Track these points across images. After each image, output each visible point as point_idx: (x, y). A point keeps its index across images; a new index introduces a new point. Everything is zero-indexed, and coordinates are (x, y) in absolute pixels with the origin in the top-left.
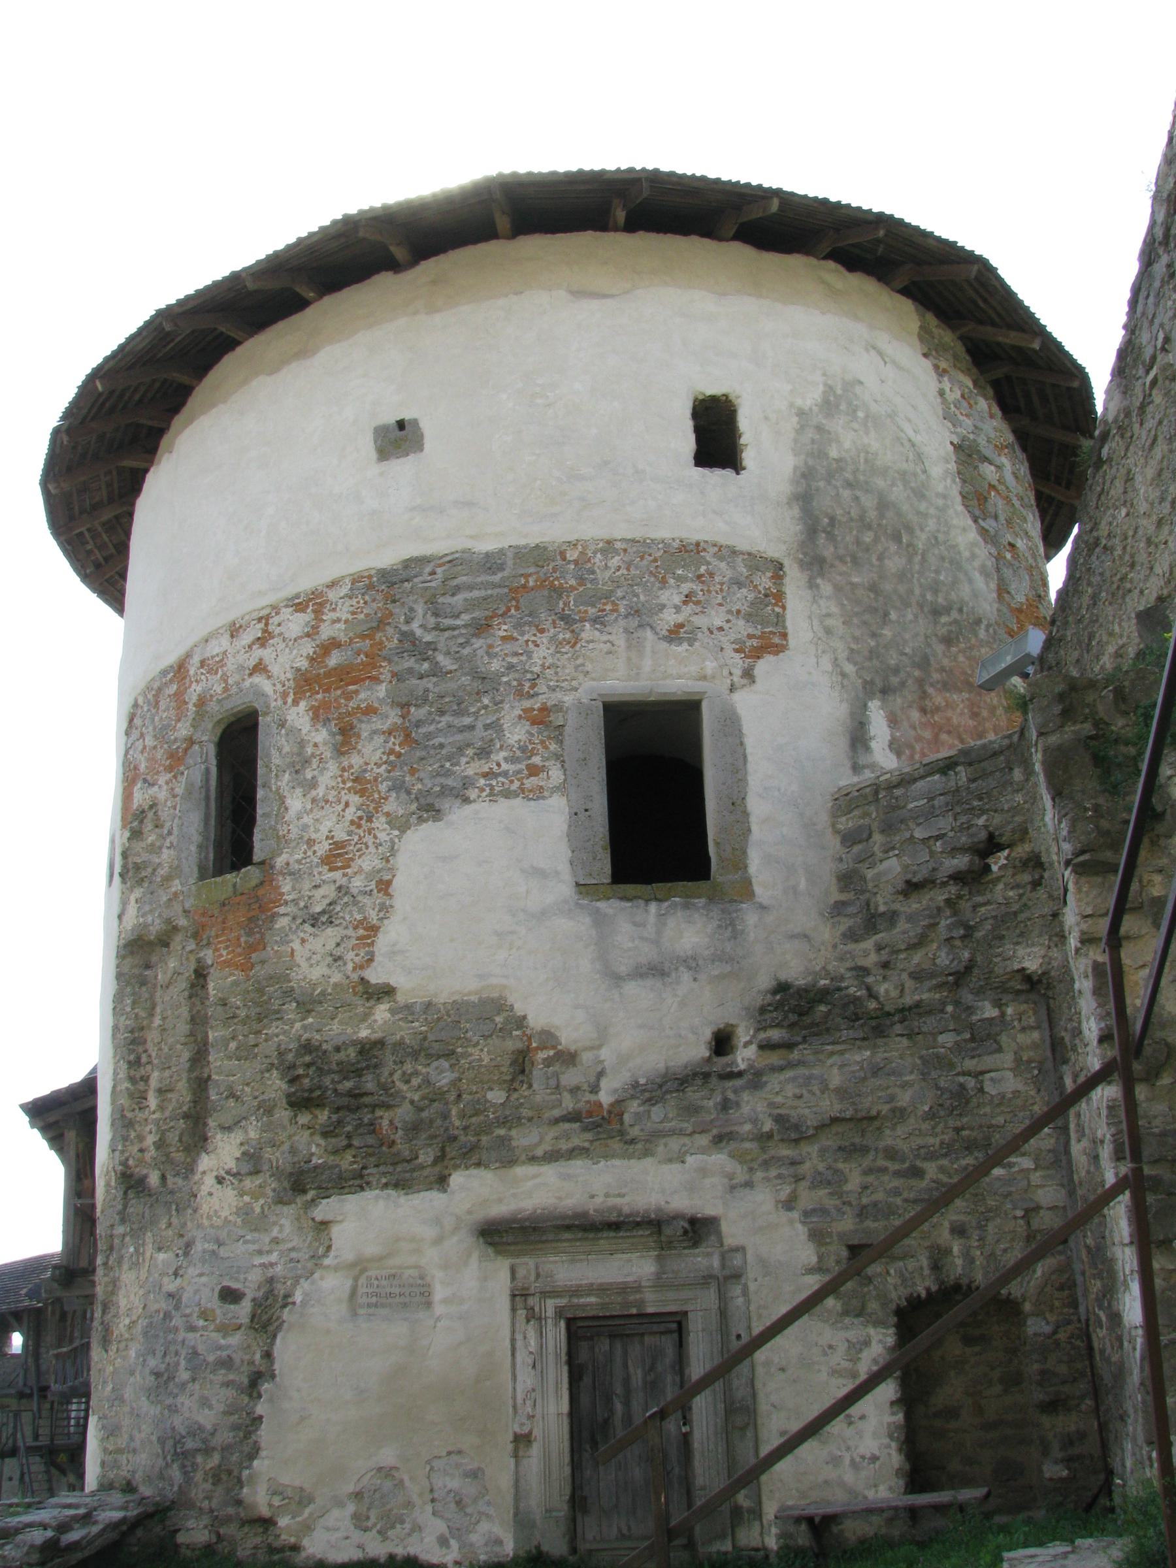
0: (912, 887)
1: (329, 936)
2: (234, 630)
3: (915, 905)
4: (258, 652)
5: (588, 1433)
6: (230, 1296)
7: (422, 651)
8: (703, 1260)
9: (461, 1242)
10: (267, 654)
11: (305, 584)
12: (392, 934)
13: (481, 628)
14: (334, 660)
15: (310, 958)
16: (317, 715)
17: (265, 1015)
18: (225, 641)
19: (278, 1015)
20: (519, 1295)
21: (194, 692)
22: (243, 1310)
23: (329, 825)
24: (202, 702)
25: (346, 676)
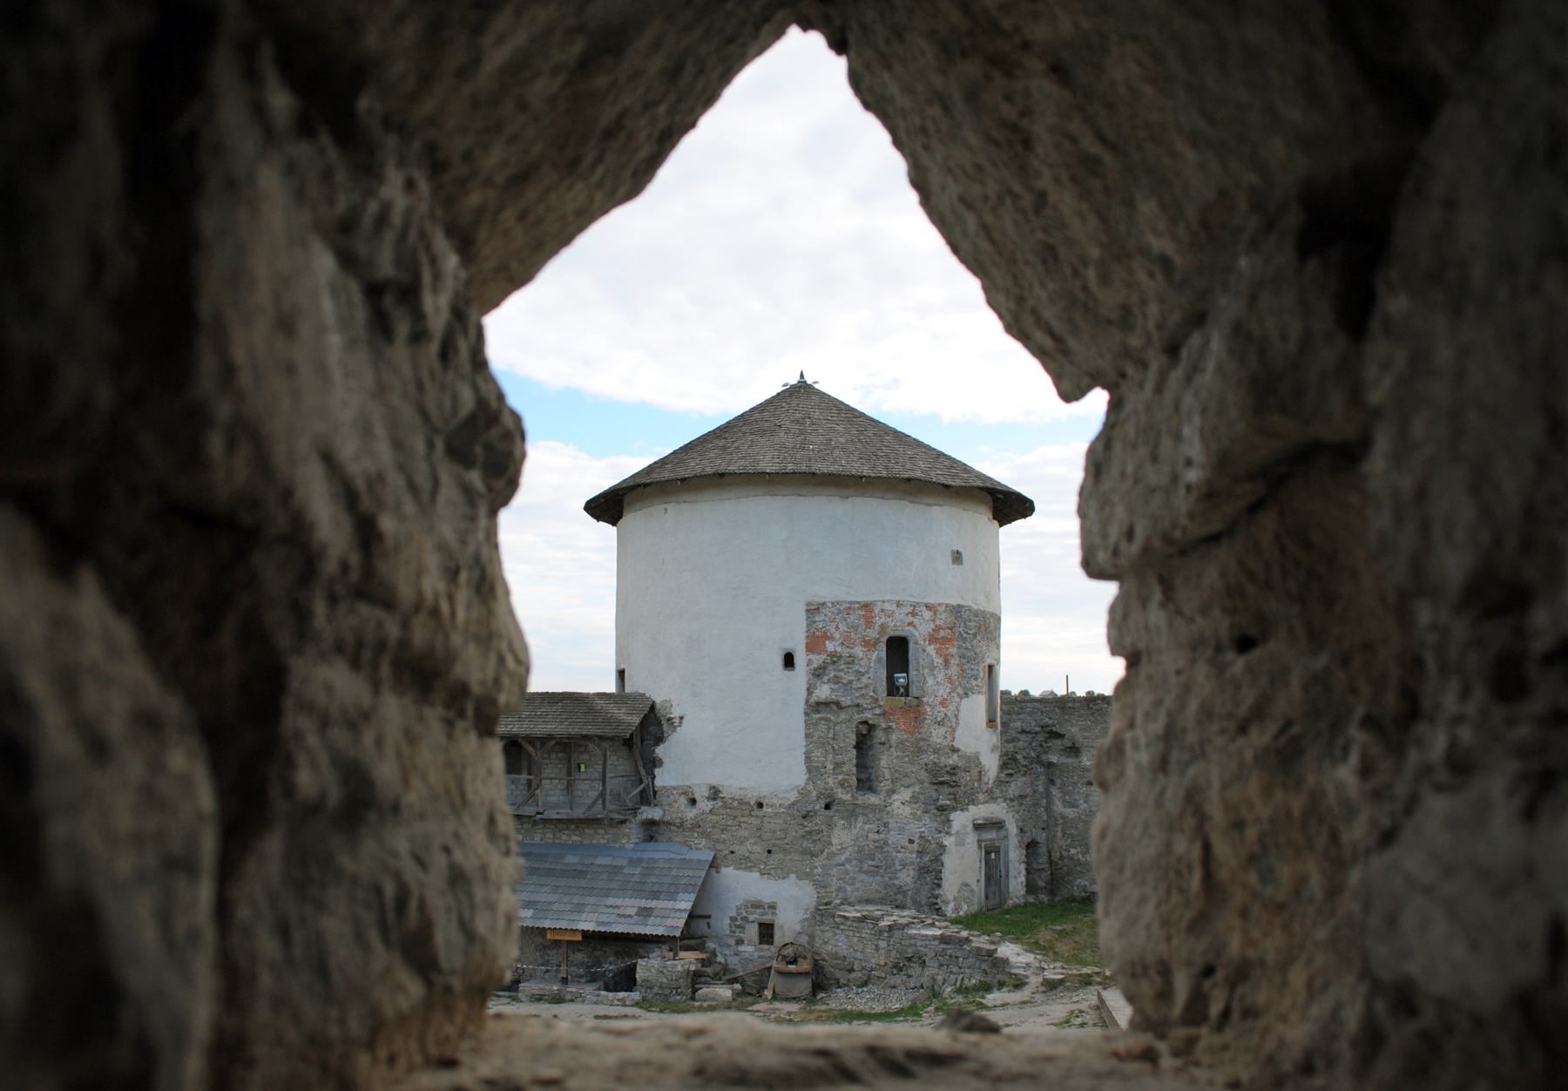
0: (1023, 732)
1: (943, 729)
2: (899, 604)
3: (1023, 737)
4: (910, 619)
5: (988, 878)
6: (911, 842)
7: (964, 640)
8: (1002, 833)
9: (970, 828)
10: (916, 620)
11: (930, 600)
12: (959, 732)
13: (975, 635)
14: (942, 633)
15: (937, 735)
16: (938, 651)
17: (920, 751)
18: (894, 607)
19: (925, 752)
20: (979, 841)
21: (878, 621)
22: (915, 846)
23: (943, 692)
24: (883, 626)
25: (945, 640)
